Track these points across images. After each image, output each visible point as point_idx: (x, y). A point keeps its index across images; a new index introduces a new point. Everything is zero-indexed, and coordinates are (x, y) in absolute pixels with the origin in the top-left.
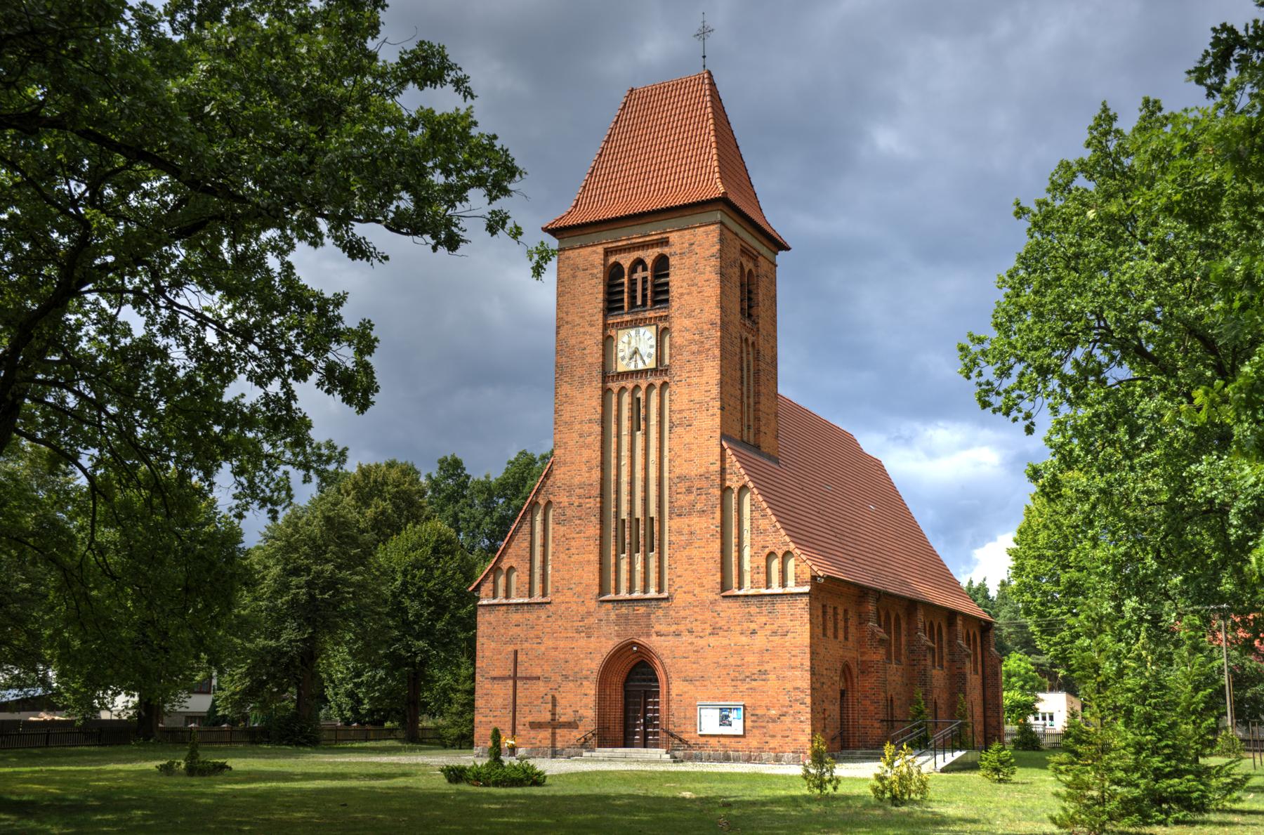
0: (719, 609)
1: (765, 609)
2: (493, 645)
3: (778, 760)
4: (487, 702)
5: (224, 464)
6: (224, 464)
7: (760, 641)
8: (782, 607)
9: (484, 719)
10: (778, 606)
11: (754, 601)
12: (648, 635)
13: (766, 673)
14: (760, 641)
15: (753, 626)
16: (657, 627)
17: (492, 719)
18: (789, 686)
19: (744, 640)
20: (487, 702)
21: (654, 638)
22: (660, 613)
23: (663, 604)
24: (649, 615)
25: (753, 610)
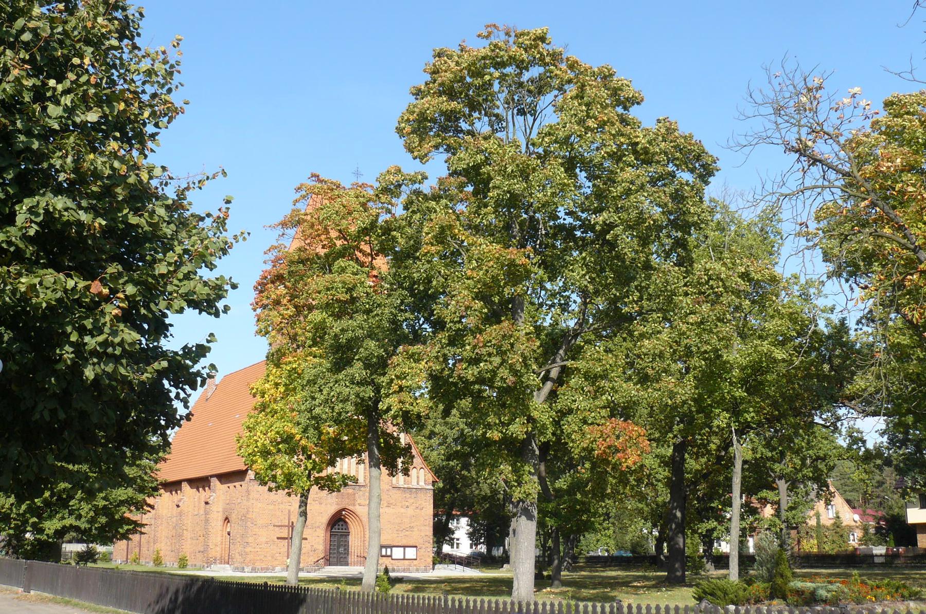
0: (391, 493)
1: (413, 496)
2: (260, 505)
3: (417, 570)
4: (255, 539)
5: (872, 448)
6: (872, 448)
7: (410, 511)
8: (421, 495)
9: (253, 550)
10: (419, 495)
11: (408, 491)
12: (354, 505)
13: (413, 527)
14: (410, 511)
15: (407, 504)
16: (359, 501)
17: (259, 550)
18: (423, 534)
19: (403, 510)
20: (255, 539)
21: (357, 506)
22: (361, 493)
23: (362, 489)
24: (354, 494)
25: (408, 495)
